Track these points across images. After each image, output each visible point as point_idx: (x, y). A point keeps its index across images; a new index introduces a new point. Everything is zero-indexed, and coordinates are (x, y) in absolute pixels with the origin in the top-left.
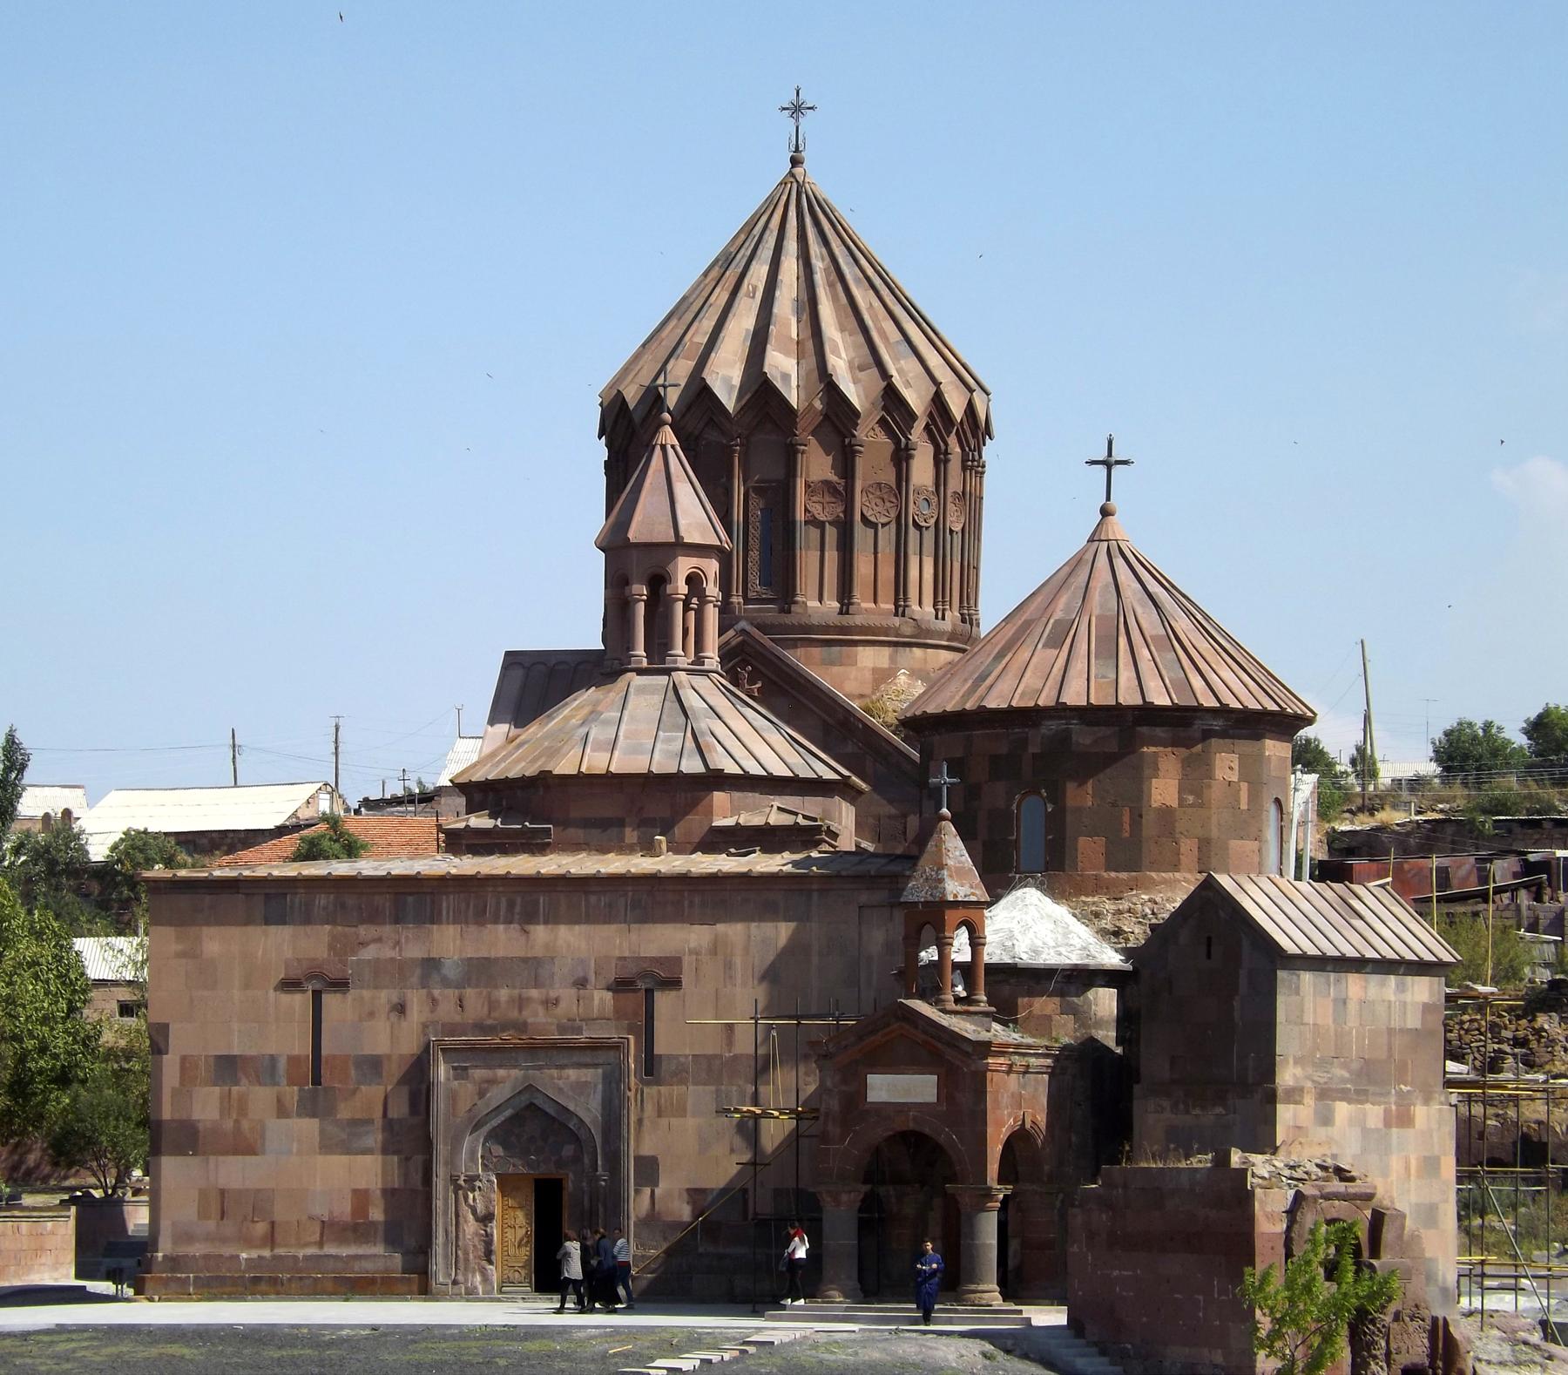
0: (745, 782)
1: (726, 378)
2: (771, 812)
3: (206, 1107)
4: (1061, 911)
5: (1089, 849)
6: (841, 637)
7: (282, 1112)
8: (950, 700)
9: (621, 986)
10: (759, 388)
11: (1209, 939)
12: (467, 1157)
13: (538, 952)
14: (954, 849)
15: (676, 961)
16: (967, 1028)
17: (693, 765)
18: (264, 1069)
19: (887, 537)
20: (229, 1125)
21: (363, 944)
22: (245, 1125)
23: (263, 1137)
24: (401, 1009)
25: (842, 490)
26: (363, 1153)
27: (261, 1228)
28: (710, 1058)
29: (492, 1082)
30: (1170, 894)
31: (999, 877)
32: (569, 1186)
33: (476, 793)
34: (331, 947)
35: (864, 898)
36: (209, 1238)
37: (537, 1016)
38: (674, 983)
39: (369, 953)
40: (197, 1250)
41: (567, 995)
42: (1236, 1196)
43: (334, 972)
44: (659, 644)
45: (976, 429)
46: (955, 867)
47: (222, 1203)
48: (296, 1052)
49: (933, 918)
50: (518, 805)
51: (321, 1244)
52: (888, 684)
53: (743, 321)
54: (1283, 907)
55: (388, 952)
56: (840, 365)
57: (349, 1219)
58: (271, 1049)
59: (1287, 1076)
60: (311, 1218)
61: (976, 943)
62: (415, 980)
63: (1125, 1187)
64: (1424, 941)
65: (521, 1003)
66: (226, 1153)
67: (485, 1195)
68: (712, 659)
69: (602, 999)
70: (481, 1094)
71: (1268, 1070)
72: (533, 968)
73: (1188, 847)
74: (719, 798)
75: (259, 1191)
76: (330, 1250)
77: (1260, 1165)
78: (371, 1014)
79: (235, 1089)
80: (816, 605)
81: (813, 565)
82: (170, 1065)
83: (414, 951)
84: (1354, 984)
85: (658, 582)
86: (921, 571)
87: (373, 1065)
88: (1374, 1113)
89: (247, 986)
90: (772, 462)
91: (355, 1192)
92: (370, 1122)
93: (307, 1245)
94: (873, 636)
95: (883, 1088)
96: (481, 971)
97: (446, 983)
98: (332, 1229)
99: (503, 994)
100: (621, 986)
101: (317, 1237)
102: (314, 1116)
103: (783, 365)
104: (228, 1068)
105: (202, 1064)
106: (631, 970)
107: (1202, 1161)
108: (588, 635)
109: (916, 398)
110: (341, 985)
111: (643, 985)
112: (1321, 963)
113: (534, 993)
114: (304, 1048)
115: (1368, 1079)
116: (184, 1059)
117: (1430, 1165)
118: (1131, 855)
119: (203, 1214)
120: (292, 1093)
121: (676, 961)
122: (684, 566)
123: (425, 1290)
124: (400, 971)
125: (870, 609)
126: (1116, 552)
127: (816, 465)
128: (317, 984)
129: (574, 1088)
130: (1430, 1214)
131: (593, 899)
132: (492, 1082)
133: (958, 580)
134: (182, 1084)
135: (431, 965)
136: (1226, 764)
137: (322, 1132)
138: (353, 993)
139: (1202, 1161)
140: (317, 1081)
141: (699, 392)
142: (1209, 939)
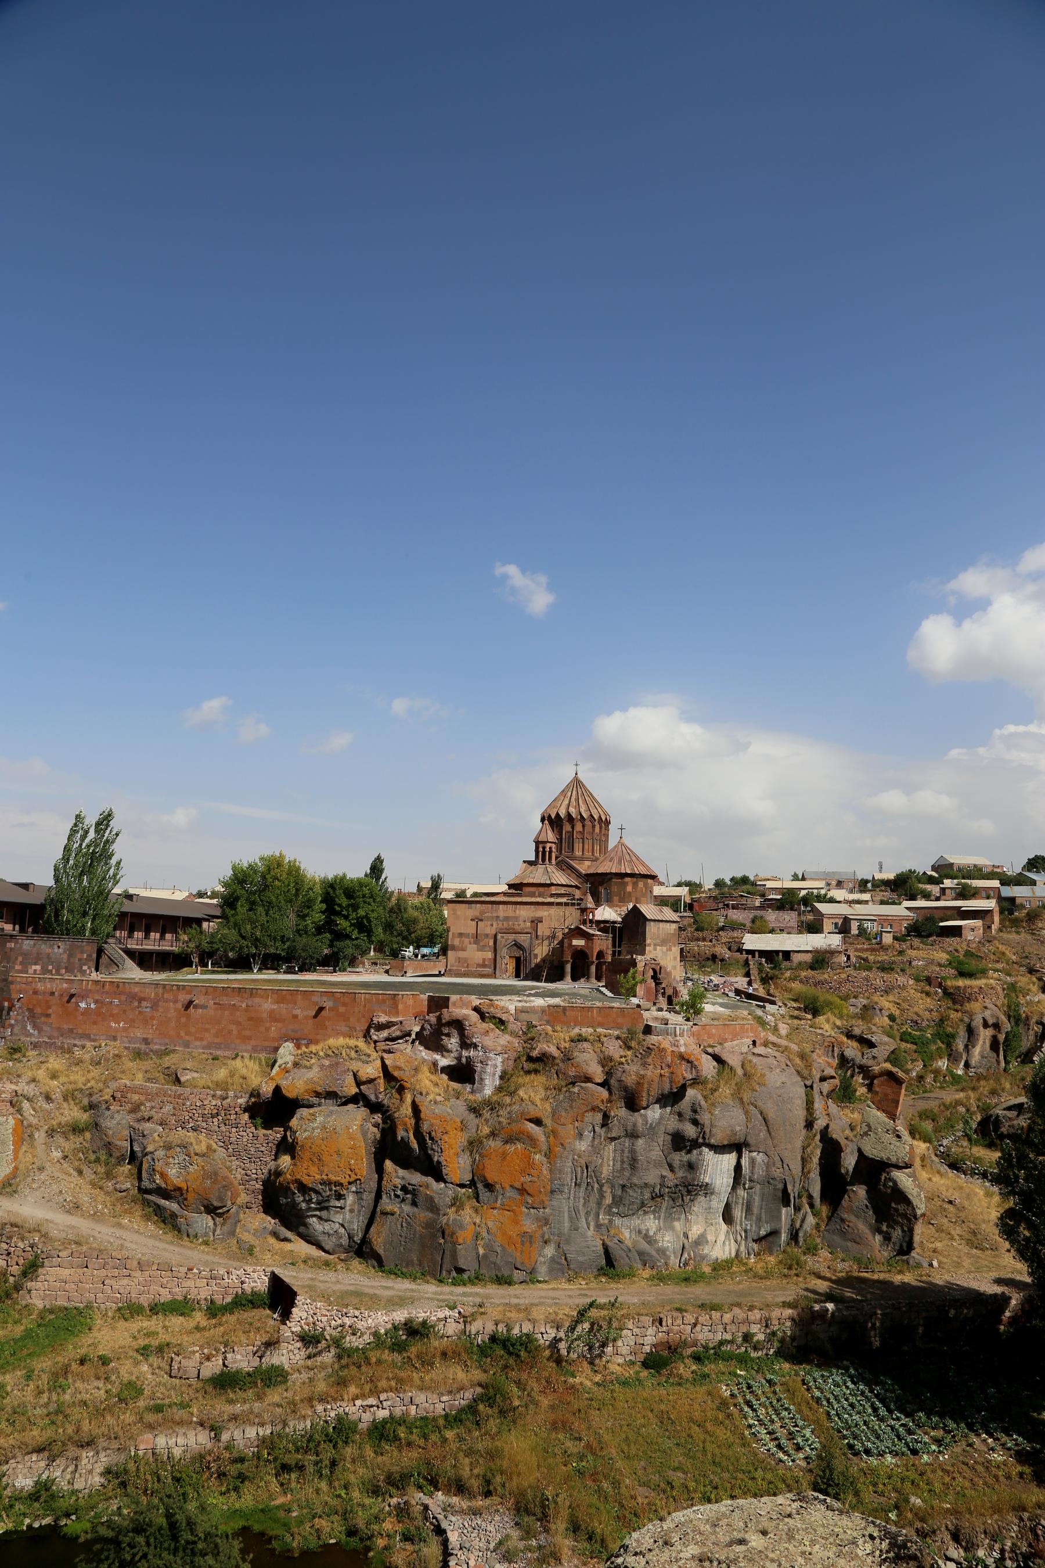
0: (558, 885)
1: (563, 813)
2: (562, 891)
3: (456, 942)
4: (610, 910)
5: (616, 899)
6: (582, 859)
8: (591, 871)
9: (532, 922)
10: (569, 815)
12: (503, 952)
14: (590, 898)
16: (591, 932)
17: (548, 882)
18: (467, 935)
19: (591, 841)
25: (582, 833)
30: (631, 906)
31: (598, 903)
33: (510, 886)
37: (516, 927)
41: (522, 923)
42: (634, 964)
44: (543, 860)
45: (607, 823)
46: (590, 902)
47: (459, 960)
49: (584, 911)
50: (516, 887)
52: (584, 867)
53: (566, 802)
54: (648, 910)
56: (582, 811)
59: (648, 941)
61: (593, 916)
64: (674, 916)
67: (507, 959)
68: (554, 861)
69: (528, 924)
71: (645, 941)
72: (516, 918)
73: (634, 899)
74: (553, 888)
77: (639, 957)
80: (578, 853)
81: (578, 846)
82: (450, 934)
84: (661, 924)
85: (544, 848)
86: (597, 848)
87: (487, 935)
88: (664, 948)
90: (569, 829)
94: (587, 859)
95: (575, 942)
96: (507, 919)
98: (478, 965)
100: (532, 922)
103: (573, 811)
104: (461, 935)
107: (629, 957)
108: (532, 857)
109: (596, 817)
111: (536, 922)
112: (655, 921)
115: (664, 942)
117: (675, 958)
118: (623, 900)
122: (548, 845)
123: (494, 975)
124: (492, 917)
125: (587, 854)
126: (623, 844)
127: (579, 827)
128: (478, 920)
129: (524, 940)
130: (674, 968)
133: (604, 849)
135: (498, 917)
136: (641, 884)
139: (629, 957)
141: (558, 814)
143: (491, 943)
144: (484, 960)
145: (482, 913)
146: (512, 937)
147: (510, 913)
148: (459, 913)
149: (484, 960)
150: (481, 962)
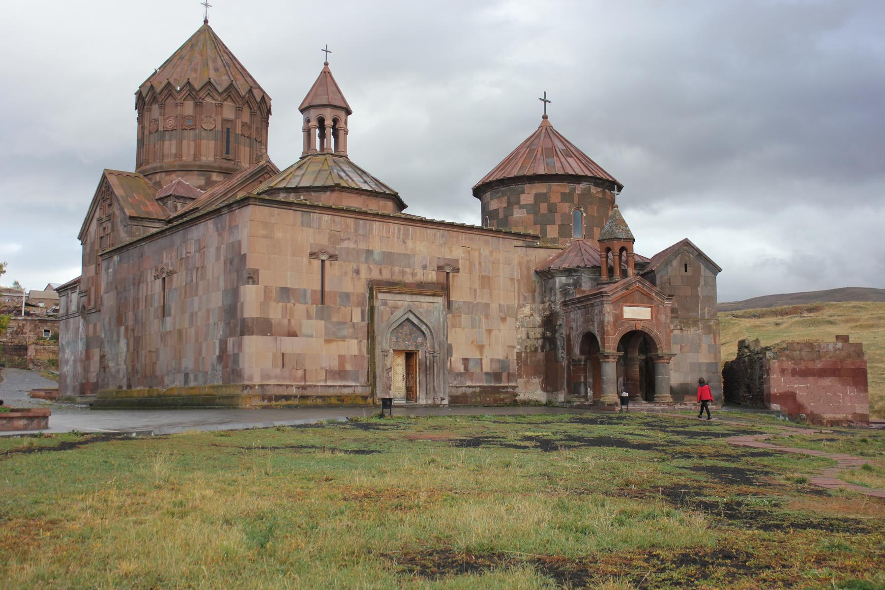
3: (275, 313)
7: (309, 317)
9: (440, 268)
11: (686, 265)
12: (385, 342)
13: (409, 252)
15: (457, 261)
20: (286, 321)
21: (342, 240)
22: (293, 321)
23: (300, 327)
24: (357, 272)
26: (343, 339)
27: (300, 373)
28: (469, 303)
29: (396, 308)
32: (420, 355)
34: (329, 240)
35: (516, 243)
36: (276, 377)
38: (456, 270)
39: (345, 245)
40: (272, 382)
43: (331, 250)
48: (315, 288)
51: (326, 380)
55: (352, 245)
57: (336, 368)
58: (303, 287)
60: (322, 368)
62: (363, 259)
63: (800, 350)
65: (403, 273)
66: (284, 335)
70: (392, 314)
72: (407, 257)
75: (299, 354)
76: (329, 383)
78: (346, 273)
79: (289, 305)
83: (363, 246)
87: (347, 296)
89: (294, 255)
91: (340, 356)
92: (345, 323)
93: (320, 381)
96: (389, 258)
97: (375, 262)
98: (331, 373)
99: (396, 269)
100: (440, 268)
101: (324, 377)
102: (322, 319)
104: (286, 293)
105: (274, 291)
106: (442, 263)
110: (333, 257)
111: (447, 269)
113: (408, 270)
114: (319, 288)
116: (266, 287)
119: (275, 366)
120: (313, 309)
121: (457, 261)
128: (324, 257)
131: (429, 231)
132: (396, 308)
134: (265, 299)
135: (369, 252)
137: (326, 327)
138: (336, 264)
140: (323, 302)
142: (686, 265)
143: (357, 318)
144: (342, 359)
145: (335, 239)
146: (404, 301)
147: (397, 248)
148: (279, 235)
149: (342, 359)
150: (335, 365)
